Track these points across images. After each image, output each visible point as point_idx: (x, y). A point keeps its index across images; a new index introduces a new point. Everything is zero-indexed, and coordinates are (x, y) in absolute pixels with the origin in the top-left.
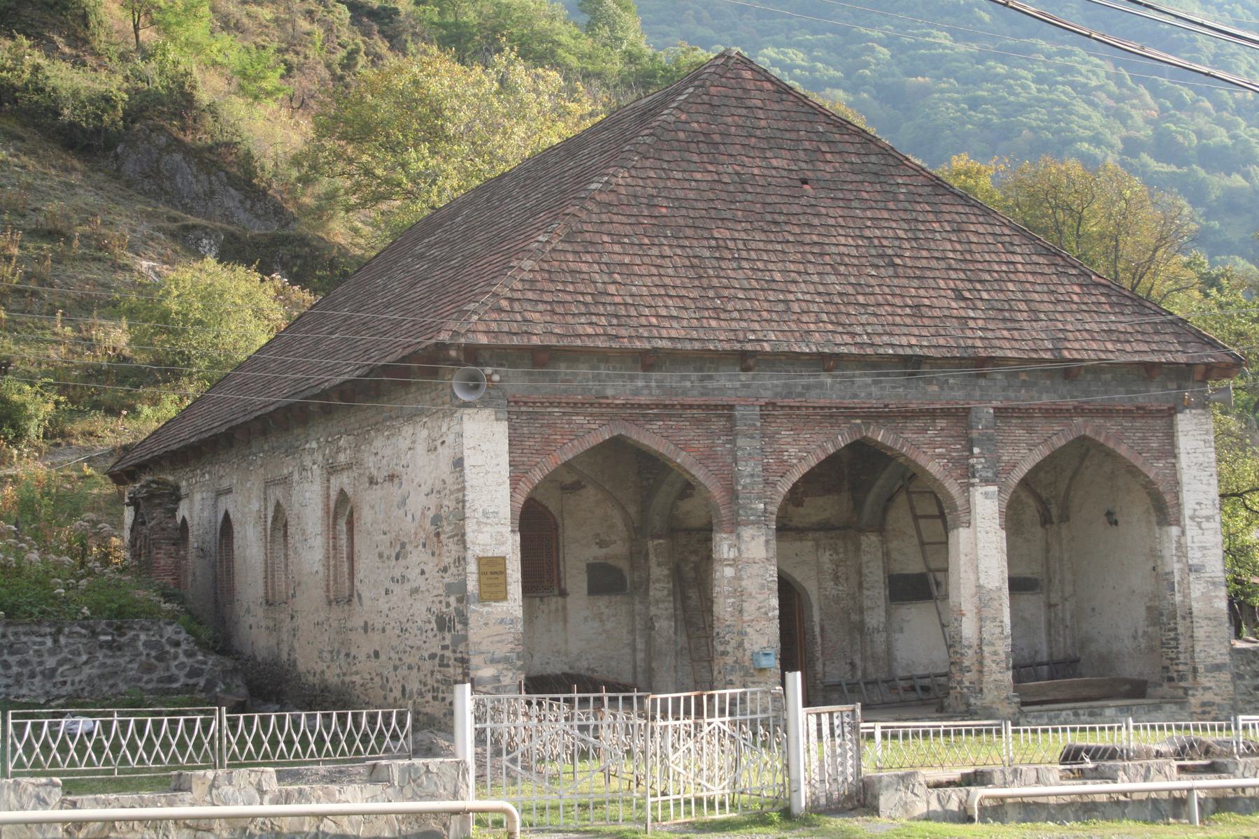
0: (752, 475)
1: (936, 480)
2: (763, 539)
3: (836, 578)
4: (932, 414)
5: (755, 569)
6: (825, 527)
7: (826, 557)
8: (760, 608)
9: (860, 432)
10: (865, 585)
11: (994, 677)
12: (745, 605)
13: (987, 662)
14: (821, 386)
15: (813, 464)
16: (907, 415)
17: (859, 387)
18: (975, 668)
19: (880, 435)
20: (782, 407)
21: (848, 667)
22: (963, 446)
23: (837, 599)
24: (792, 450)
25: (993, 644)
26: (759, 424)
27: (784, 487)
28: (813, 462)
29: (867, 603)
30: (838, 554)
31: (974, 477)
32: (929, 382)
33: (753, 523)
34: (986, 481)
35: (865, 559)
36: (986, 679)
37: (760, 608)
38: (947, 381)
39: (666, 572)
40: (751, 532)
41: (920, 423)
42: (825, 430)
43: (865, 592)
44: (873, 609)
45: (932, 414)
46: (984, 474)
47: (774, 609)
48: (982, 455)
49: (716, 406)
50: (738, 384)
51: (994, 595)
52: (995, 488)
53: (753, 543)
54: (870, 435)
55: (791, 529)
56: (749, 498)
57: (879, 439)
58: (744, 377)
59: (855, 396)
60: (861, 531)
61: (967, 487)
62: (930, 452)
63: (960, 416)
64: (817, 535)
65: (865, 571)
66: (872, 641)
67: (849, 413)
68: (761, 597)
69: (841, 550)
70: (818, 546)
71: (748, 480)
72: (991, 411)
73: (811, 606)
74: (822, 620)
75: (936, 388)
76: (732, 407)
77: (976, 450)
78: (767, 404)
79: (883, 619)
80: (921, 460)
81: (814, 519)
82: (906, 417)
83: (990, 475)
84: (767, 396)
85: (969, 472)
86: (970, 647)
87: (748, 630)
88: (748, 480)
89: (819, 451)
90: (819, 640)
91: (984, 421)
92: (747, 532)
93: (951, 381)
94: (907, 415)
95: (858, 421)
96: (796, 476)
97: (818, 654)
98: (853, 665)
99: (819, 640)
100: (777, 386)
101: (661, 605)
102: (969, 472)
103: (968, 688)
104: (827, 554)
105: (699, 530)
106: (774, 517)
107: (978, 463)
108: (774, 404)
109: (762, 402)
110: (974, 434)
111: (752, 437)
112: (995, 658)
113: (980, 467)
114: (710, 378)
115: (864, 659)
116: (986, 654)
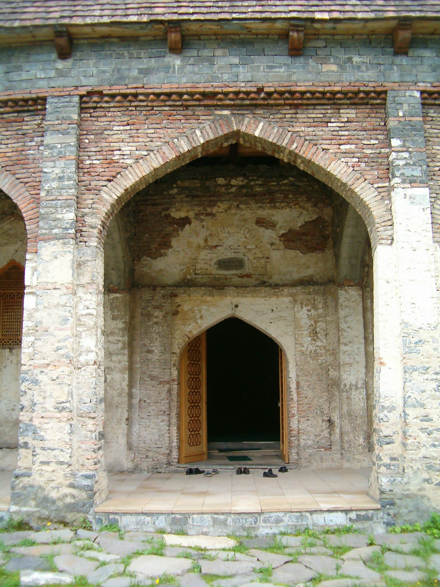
0: (61, 178)
1: (345, 185)
2: (69, 257)
3: (314, 334)
4: (331, 100)
5: (56, 297)
6: (306, 282)
7: (303, 314)
8: (58, 349)
9: (229, 124)
10: (342, 341)
11: (423, 452)
12: (38, 344)
13: (413, 430)
14: (167, 68)
15: (156, 165)
16: (293, 101)
17: (221, 67)
18: (398, 439)
19: (260, 128)
20: (113, 96)
21: (325, 425)
22: (381, 141)
23: (315, 355)
24: (126, 149)
25: (422, 406)
26: (75, 117)
27: (112, 193)
28: (156, 162)
29: (343, 358)
30: (316, 309)
31: (394, 176)
32: (325, 61)
33: (57, 238)
34: (412, 181)
35: (342, 313)
36: (409, 455)
37: (58, 349)
38: (350, 60)
39: (121, 325)
40: (55, 248)
41: (317, 114)
42: (178, 124)
43: (343, 348)
44: (351, 365)
45: (331, 100)
46: (408, 172)
47: (89, 351)
48: (405, 149)
49: (26, 101)
50: (52, 74)
51: (423, 335)
52: (425, 191)
53: (56, 262)
54: (243, 129)
55: (270, 286)
56: (56, 207)
57: (257, 134)
58: (60, 65)
59: (215, 78)
60: (341, 285)
61: (386, 194)
62: (333, 149)
63: (371, 100)
64: (294, 290)
65: (343, 326)
66: (348, 398)
67: (208, 100)
68: (62, 335)
69: (320, 306)
70: (295, 301)
71: (55, 184)
72: (417, 95)
73: (287, 362)
74: (298, 376)
75: (334, 68)
76: (44, 99)
77: (395, 142)
78: (90, 94)
79: (362, 376)
80: (320, 160)
81: (296, 276)
82: (297, 106)
83: (417, 172)
84: (90, 83)
85: (388, 171)
86: (392, 409)
87: (40, 377)
88: (55, 184)
89: (165, 149)
90: (295, 396)
91: (405, 107)
92: (47, 250)
93: (356, 59)
94: (293, 101)
95: (226, 112)
96: (130, 179)
97: (294, 411)
98: (330, 422)
99: (295, 396)
100: (104, 72)
101: (114, 358)
102: (388, 171)
103: (388, 466)
104: (305, 309)
105: (163, 287)
106: (96, 231)
107: (399, 159)
108: (101, 94)
109: (83, 91)
110: (392, 123)
111: (65, 133)
112: (425, 424)
113: (402, 163)
114: (19, 68)
115: (341, 417)
116: (410, 419)
